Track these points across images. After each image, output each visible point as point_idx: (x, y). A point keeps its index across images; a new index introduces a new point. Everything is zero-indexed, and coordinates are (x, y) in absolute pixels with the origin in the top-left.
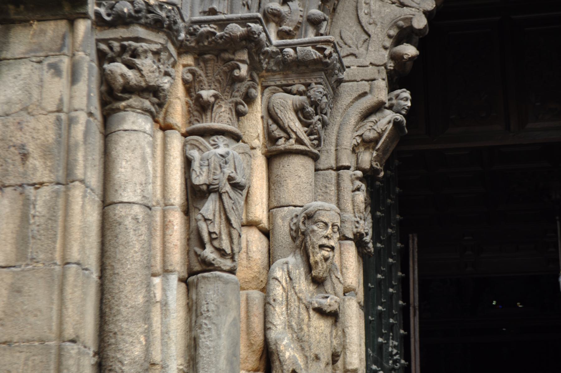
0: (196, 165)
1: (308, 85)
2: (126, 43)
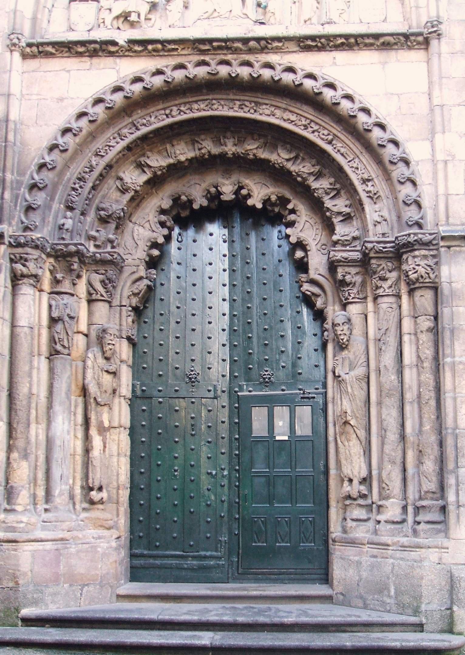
0: (53, 308)
1: (106, 271)
2: (22, 255)
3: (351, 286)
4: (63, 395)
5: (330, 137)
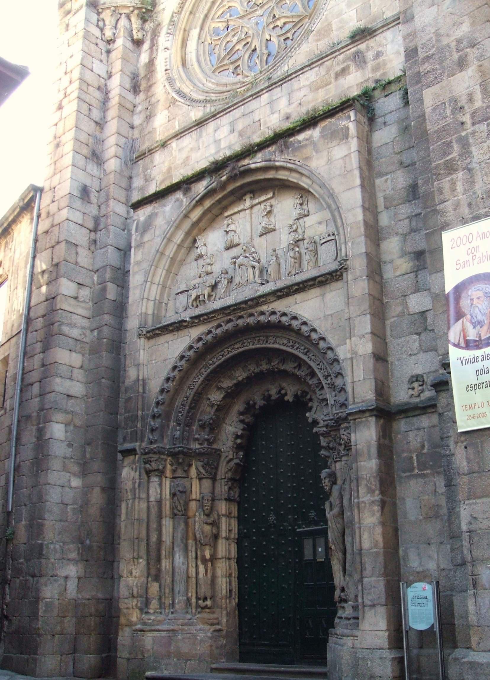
4: (179, 540)
5: (306, 350)
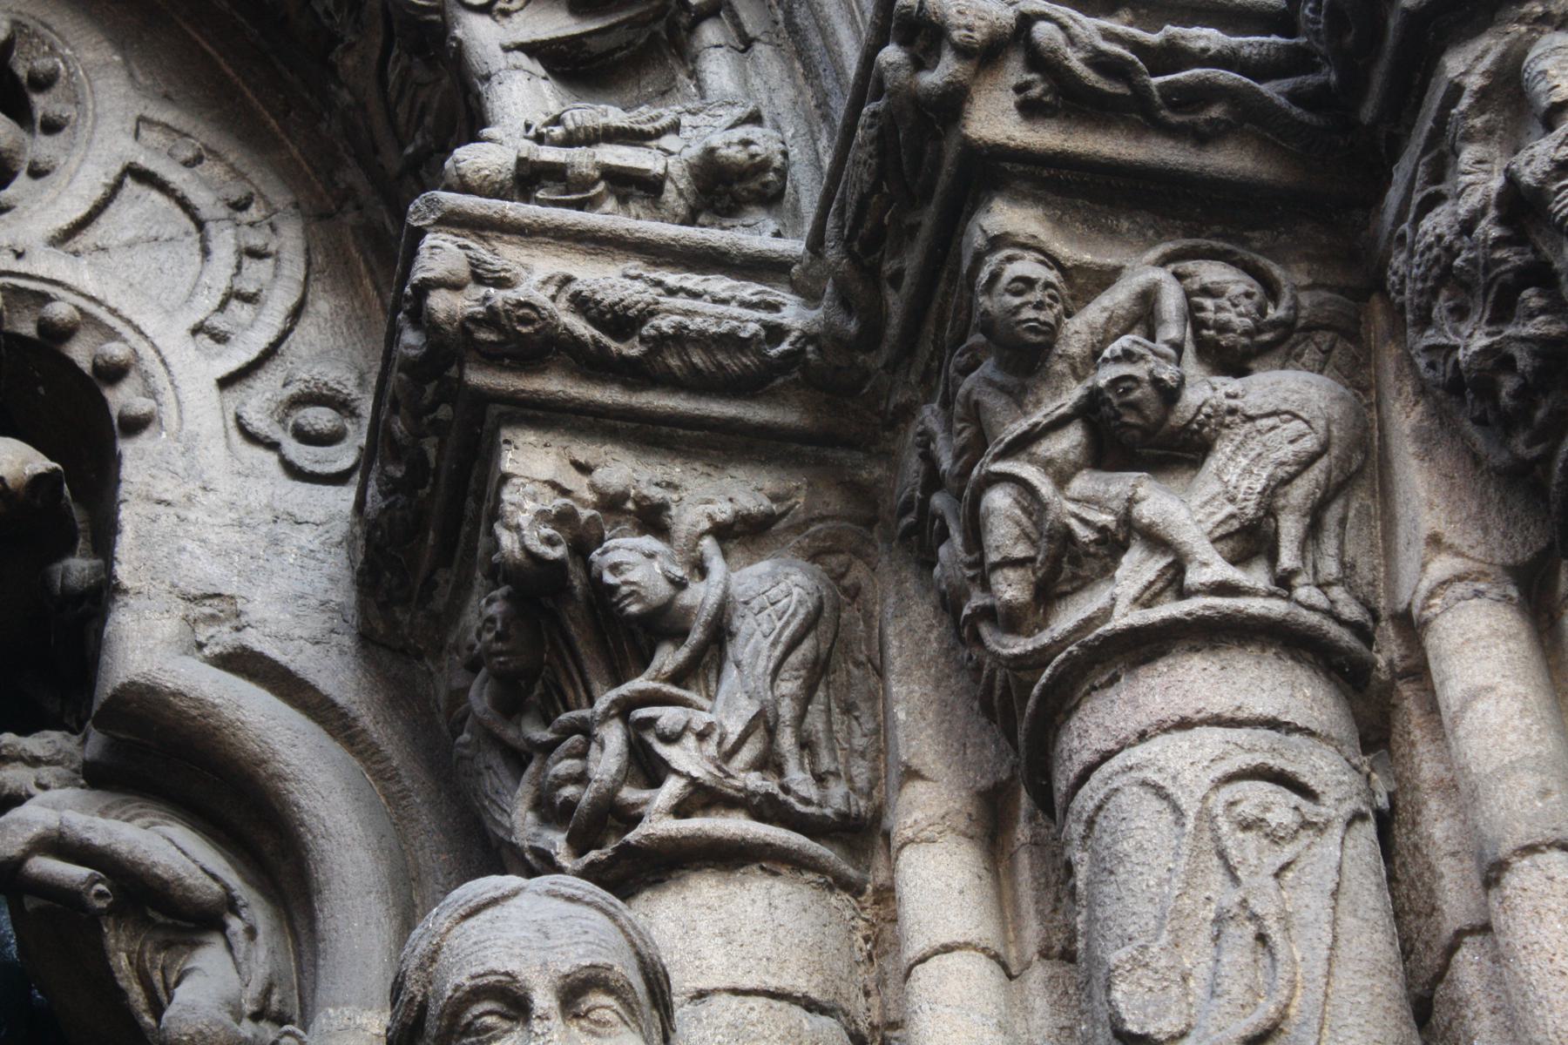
3: (668, 658)
